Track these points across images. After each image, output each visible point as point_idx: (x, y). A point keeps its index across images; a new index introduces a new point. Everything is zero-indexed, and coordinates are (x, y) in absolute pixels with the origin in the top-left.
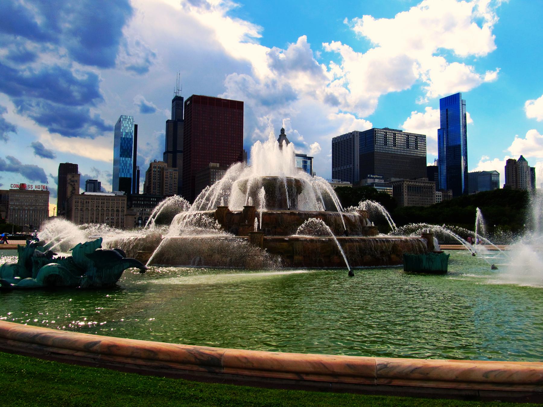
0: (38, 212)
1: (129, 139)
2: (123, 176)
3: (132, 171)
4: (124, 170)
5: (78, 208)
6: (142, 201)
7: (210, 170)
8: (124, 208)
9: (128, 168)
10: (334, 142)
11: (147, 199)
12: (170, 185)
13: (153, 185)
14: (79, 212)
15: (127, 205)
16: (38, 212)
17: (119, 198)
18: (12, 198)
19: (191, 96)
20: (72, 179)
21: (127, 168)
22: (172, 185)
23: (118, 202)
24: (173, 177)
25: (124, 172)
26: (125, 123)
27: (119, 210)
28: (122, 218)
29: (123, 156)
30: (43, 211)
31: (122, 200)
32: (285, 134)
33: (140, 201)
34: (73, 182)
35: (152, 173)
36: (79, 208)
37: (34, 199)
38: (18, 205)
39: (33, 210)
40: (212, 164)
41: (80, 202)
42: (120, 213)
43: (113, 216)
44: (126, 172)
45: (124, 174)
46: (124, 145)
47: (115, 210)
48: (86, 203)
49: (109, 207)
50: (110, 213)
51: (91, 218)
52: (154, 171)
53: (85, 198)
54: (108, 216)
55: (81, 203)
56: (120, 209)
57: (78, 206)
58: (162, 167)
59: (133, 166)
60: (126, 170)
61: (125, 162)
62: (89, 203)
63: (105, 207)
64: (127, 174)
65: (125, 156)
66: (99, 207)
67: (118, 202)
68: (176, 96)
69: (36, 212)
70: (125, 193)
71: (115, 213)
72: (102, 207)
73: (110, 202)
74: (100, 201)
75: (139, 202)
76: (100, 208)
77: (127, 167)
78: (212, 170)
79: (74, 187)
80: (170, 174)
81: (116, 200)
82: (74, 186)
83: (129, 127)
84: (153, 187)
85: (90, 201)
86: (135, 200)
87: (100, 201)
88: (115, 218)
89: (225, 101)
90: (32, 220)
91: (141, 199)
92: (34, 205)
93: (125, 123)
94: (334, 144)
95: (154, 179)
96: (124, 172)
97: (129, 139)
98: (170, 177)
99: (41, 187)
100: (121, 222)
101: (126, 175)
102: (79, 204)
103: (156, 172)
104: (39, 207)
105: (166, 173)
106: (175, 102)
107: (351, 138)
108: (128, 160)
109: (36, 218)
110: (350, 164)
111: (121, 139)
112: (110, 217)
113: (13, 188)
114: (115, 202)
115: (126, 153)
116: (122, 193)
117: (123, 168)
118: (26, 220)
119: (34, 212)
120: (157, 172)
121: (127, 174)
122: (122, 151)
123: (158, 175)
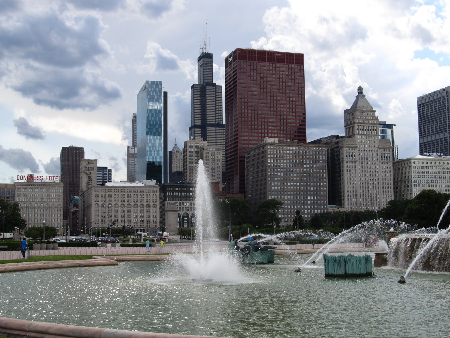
0: (50, 210)
1: (157, 111)
2: (151, 160)
3: (162, 154)
4: (153, 152)
5: (98, 204)
6: (178, 191)
7: (266, 147)
8: (156, 202)
9: (157, 149)
10: (420, 103)
11: (185, 189)
12: (212, 169)
13: (190, 170)
14: (100, 208)
15: (160, 198)
16: (50, 210)
17: (149, 189)
18: (19, 193)
19: (234, 50)
20: (88, 166)
21: (156, 149)
22: (214, 169)
23: (148, 194)
24: (216, 158)
25: (153, 154)
26: (151, 90)
27: (150, 205)
28: (153, 216)
29: (150, 134)
30: (56, 209)
31: (153, 192)
32: (364, 93)
33: (176, 191)
34: (89, 170)
35: (188, 154)
36: (100, 203)
37: (45, 193)
38: (26, 202)
39: (44, 208)
40: (267, 140)
41: (100, 196)
43: (143, 213)
44: (154, 155)
45: (153, 157)
46: (152, 120)
47: (145, 205)
48: (109, 196)
49: (137, 202)
50: (139, 209)
51: (115, 216)
52: (190, 152)
53: (107, 191)
54: (137, 213)
55: (102, 197)
56: (151, 204)
57: (98, 201)
58: (200, 146)
59: (163, 147)
60: (154, 151)
61: (153, 141)
62: (111, 196)
63: (132, 201)
65: (153, 134)
66: (124, 201)
67: (148, 194)
68: (203, 53)
69: (48, 211)
70: (157, 182)
72: (128, 201)
73: (139, 194)
74: (125, 193)
75: (175, 193)
76: (126, 203)
77: (156, 147)
78: (269, 147)
79: (90, 177)
80: (212, 155)
81: (145, 191)
82: (90, 175)
83: (157, 95)
84: (190, 173)
85: (113, 194)
86: (170, 191)
87: (126, 194)
88: (146, 215)
89: (280, 55)
91: (177, 189)
92: (45, 202)
93: (151, 90)
94: (420, 105)
95: (190, 162)
96: (153, 154)
97: (157, 111)
98: (212, 159)
99: (52, 177)
100: (153, 221)
101: (154, 158)
102: (100, 198)
103: (192, 152)
104: (50, 204)
105: (206, 153)
106: (202, 61)
107: (444, 97)
108: (157, 138)
109: (48, 218)
110: (444, 131)
111: (147, 112)
112: (139, 215)
113: (20, 181)
114: (145, 194)
115: (154, 130)
116: (153, 182)
117: (151, 149)
118: (36, 220)
119: (45, 209)
120: (194, 152)
121: (156, 157)
123: (196, 156)
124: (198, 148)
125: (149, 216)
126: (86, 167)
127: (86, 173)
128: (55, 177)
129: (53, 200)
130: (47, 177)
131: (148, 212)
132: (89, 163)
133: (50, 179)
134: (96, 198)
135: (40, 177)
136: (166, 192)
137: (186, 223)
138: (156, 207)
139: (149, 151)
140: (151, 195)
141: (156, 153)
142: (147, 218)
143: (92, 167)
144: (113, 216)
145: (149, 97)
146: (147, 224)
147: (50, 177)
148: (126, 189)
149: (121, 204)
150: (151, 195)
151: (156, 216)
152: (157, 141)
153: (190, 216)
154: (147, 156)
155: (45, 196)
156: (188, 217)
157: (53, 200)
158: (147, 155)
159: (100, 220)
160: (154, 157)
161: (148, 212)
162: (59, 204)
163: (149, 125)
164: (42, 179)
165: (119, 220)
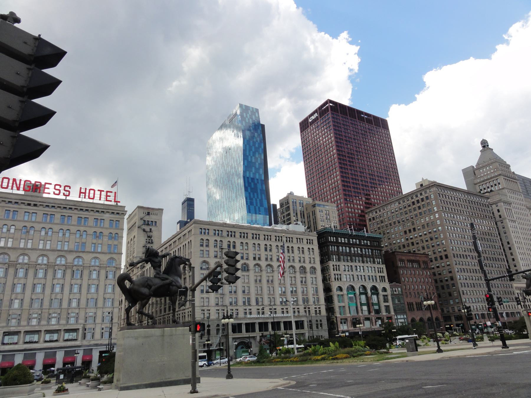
4: (254, 201)
9: (259, 196)
20: (147, 218)
21: (258, 197)
30: (103, 272)
34: (148, 225)
38: (9, 248)
39: (66, 267)
42: (309, 276)
46: (250, 155)
47: (297, 269)
51: (244, 292)
55: (216, 246)
56: (308, 266)
60: (256, 200)
64: (259, 208)
77: (258, 195)
80: (326, 214)
99: (97, 193)
106: (186, 203)
119: (69, 272)
121: (259, 208)
122: (246, 165)
126: (145, 219)
127: (144, 230)
128: (104, 194)
130: (83, 191)
131: (304, 282)
132: (148, 214)
133: (92, 196)
134: (202, 248)
135: (62, 188)
141: (258, 202)
143: (154, 221)
146: (305, 308)
147: (92, 192)
149: (255, 265)
155: (73, 237)
156: (366, 294)
161: (304, 282)
162: (112, 258)
163: (246, 161)
164: (67, 193)
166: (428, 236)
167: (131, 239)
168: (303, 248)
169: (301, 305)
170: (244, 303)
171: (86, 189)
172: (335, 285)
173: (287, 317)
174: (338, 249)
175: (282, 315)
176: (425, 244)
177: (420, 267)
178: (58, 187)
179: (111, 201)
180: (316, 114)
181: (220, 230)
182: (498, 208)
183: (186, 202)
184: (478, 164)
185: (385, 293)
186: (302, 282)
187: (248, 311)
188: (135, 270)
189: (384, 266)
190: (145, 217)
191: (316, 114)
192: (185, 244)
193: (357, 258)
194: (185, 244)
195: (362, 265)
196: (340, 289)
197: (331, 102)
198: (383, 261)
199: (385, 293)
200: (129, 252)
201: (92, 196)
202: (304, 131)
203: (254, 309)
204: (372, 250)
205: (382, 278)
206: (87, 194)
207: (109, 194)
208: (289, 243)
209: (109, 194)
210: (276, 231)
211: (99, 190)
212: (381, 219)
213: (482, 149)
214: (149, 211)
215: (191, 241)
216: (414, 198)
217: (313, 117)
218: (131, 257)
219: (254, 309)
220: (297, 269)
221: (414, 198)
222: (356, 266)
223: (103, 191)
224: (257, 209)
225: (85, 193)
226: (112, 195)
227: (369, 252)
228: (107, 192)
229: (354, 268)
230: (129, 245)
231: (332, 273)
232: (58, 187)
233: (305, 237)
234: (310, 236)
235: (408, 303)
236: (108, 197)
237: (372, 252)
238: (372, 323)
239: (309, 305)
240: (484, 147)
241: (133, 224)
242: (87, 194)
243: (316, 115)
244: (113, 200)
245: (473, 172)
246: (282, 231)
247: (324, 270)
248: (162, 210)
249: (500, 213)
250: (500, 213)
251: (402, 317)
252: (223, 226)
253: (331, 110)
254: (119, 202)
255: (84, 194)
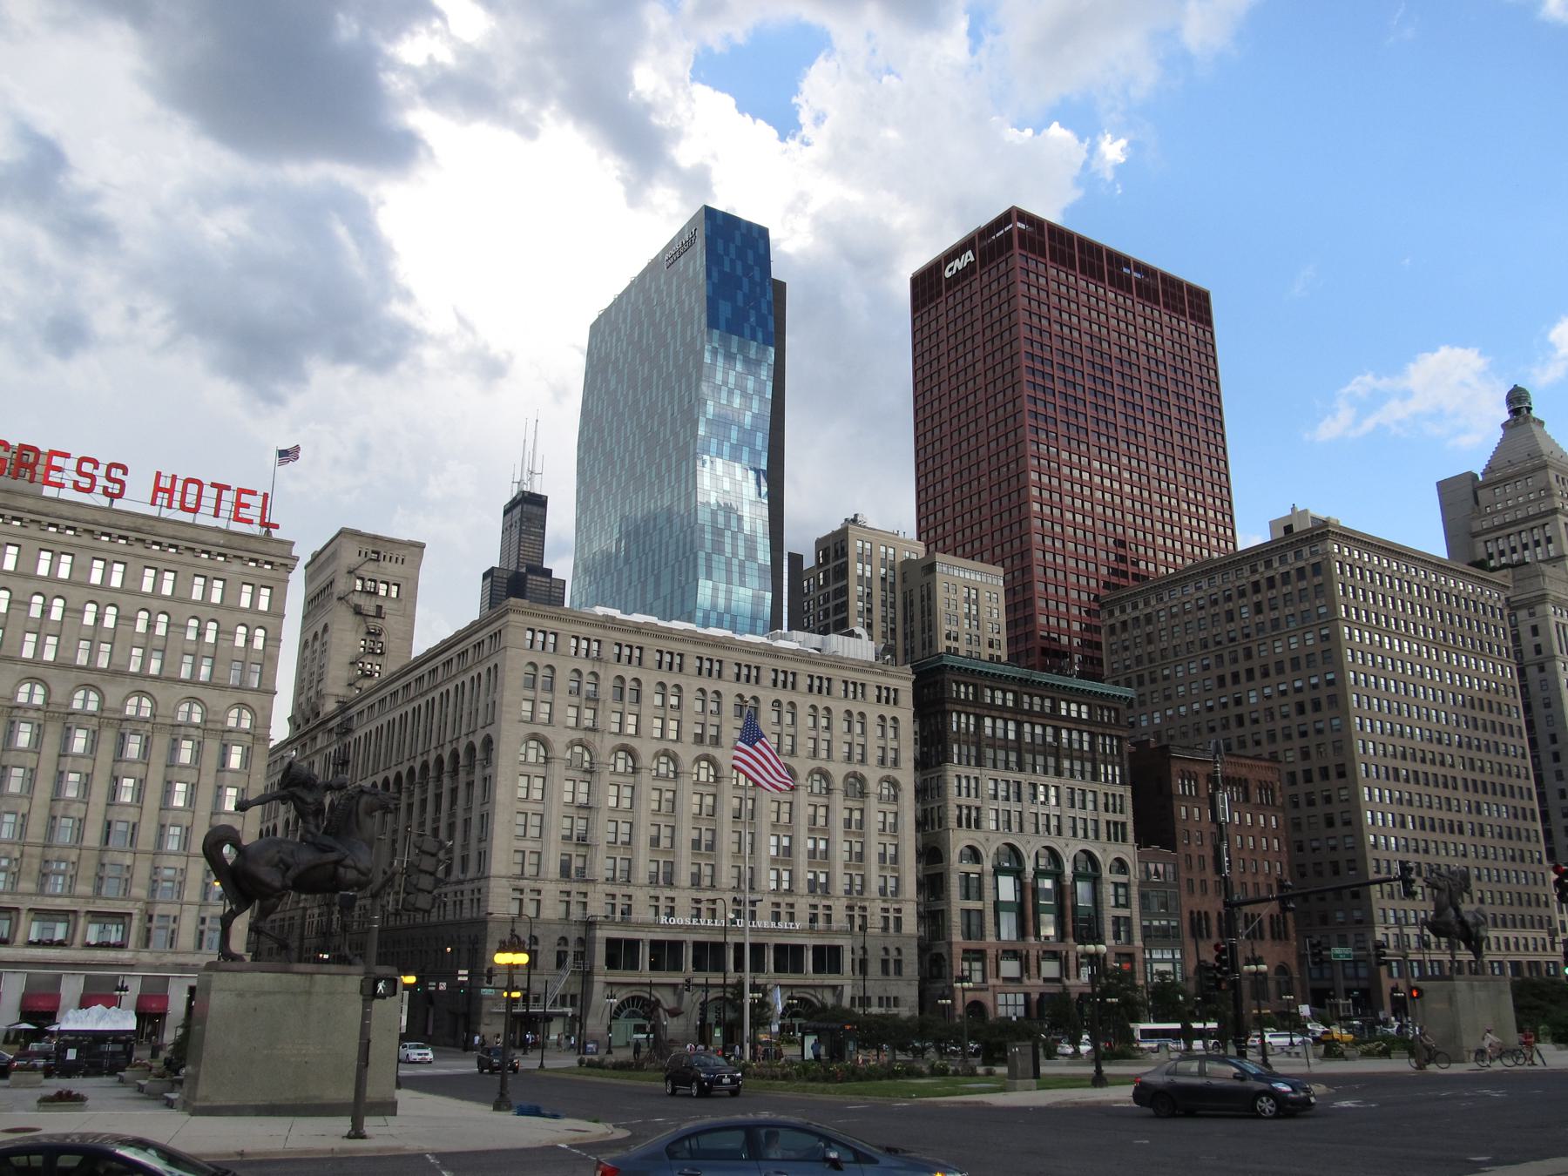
4: (728, 540)
47: (838, 782)
51: (655, 841)
56: (873, 773)
58: (899, 560)
64: (742, 565)
65: (726, 449)
66: (716, 741)
71: (838, 800)
73: (804, 701)
74: (721, 686)
79: (374, 634)
80: (968, 599)
82: (374, 623)
86: (964, 706)
90: (80, 834)
93: (727, 253)
96: (728, 549)
99: (210, 493)
100: (883, 891)
106: (517, 511)
117: (721, 519)
121: (742, 565)
124: (892, 568)
125: (861, 856)
127: (358, 611)
128: (228, 496)
129: (195, 668)
131: (858, 827)
132: (377, 557)
133: (191, 500)
135: (102, 470)
136: (948, 706)
137: (1047, 910)
138: (896, 797)
139: (708, 529)
140: (872, 719)
142: (846, 866)
144: (643, 840)
145: (715, 274)
146: (850, 908)
147: (192, 488)
148: (730, 657)
150: (872, 719)
151: (895, 859)
152: (745, 492)
153: (1068, 869)
154: (702, 555)
156: (1057, 877)
157: (195, 668)
158: (702, 547)
159: (552, 867)
160: (735, 562)
164: (116, 488)
165: (684, 876)
166: (1292, 699)
167: (316, 635)
168: (862, 715)
169: (838, 898)
170: (654, 880)
171: (174, 478)
172: (958, 840)
173: (789, 931)
174: (979, 725)
175: (773, 925)
176: (1280, 724)
177: (1247, 799)
178: (87, 467)
179: (250, 522)
180: (970, 253)
181: (593, 638)
182: (1533, 621)
183: (519, 509)
184: (1489, 469)
185: (1122, 879)
186: (848, 823)
187: (662, 903)
188: (320, 735)
189: (1127, 792)
190: (366, 567)
191: (970, 253)
192: (479, 675)
193: (1040, 760)
194: (479, 675)
195: (1056, 781)
196: (974, 855)
197: (1023, 216)
198: (1127, 772)
199: (1122, 879)
200: (305, 675)
201: (191, 500)
202: (924, 305)
203: (684, 899)
204: (1093, 735)
205: (1116, 832)
206: (177, 496)
207: (245, 498)
208: (819, 696)
209: (245, 498)
210: (776, 653)
211: (214, 485)
212: (1149, 629)
213: (1507, 417)
214: (378, 549)
215: (496, 666)
216: (1261, 569)
217: (958, 264)
218: (312, 693)
219: (684, 899)
220: (838, 782)
221: (1261, 569)
222: (1035, 786)
223: (228, 488)
224: (735, 569)
225: (171, 491)
226: (256, 501)
227: (1081, 742)
228: (241, 491)
229: (1026, 791)
230: (308, 652)
231: (954, 799)
232: (87, 467)
233: (872, 680)
234: (892, 676)
235: (1192, 913)
236: (242, 510)
237: (1092, 744)
238: (1064, 968)
239: (865, 900)
240: (1515, 412)
241: (324, 585)
242: (177, 496)
243: (969, 256)
244: (257, 520)
245: (1471, 495)
246: (797, 656)
247: (929, 791)
248: (422, 546)
249: (1538, 640)
250: (1538, 640)
251: (1168, 956)
252: (605, 627)
253: (1022, 246)
254: (276, 527)
255: (166, 495)
